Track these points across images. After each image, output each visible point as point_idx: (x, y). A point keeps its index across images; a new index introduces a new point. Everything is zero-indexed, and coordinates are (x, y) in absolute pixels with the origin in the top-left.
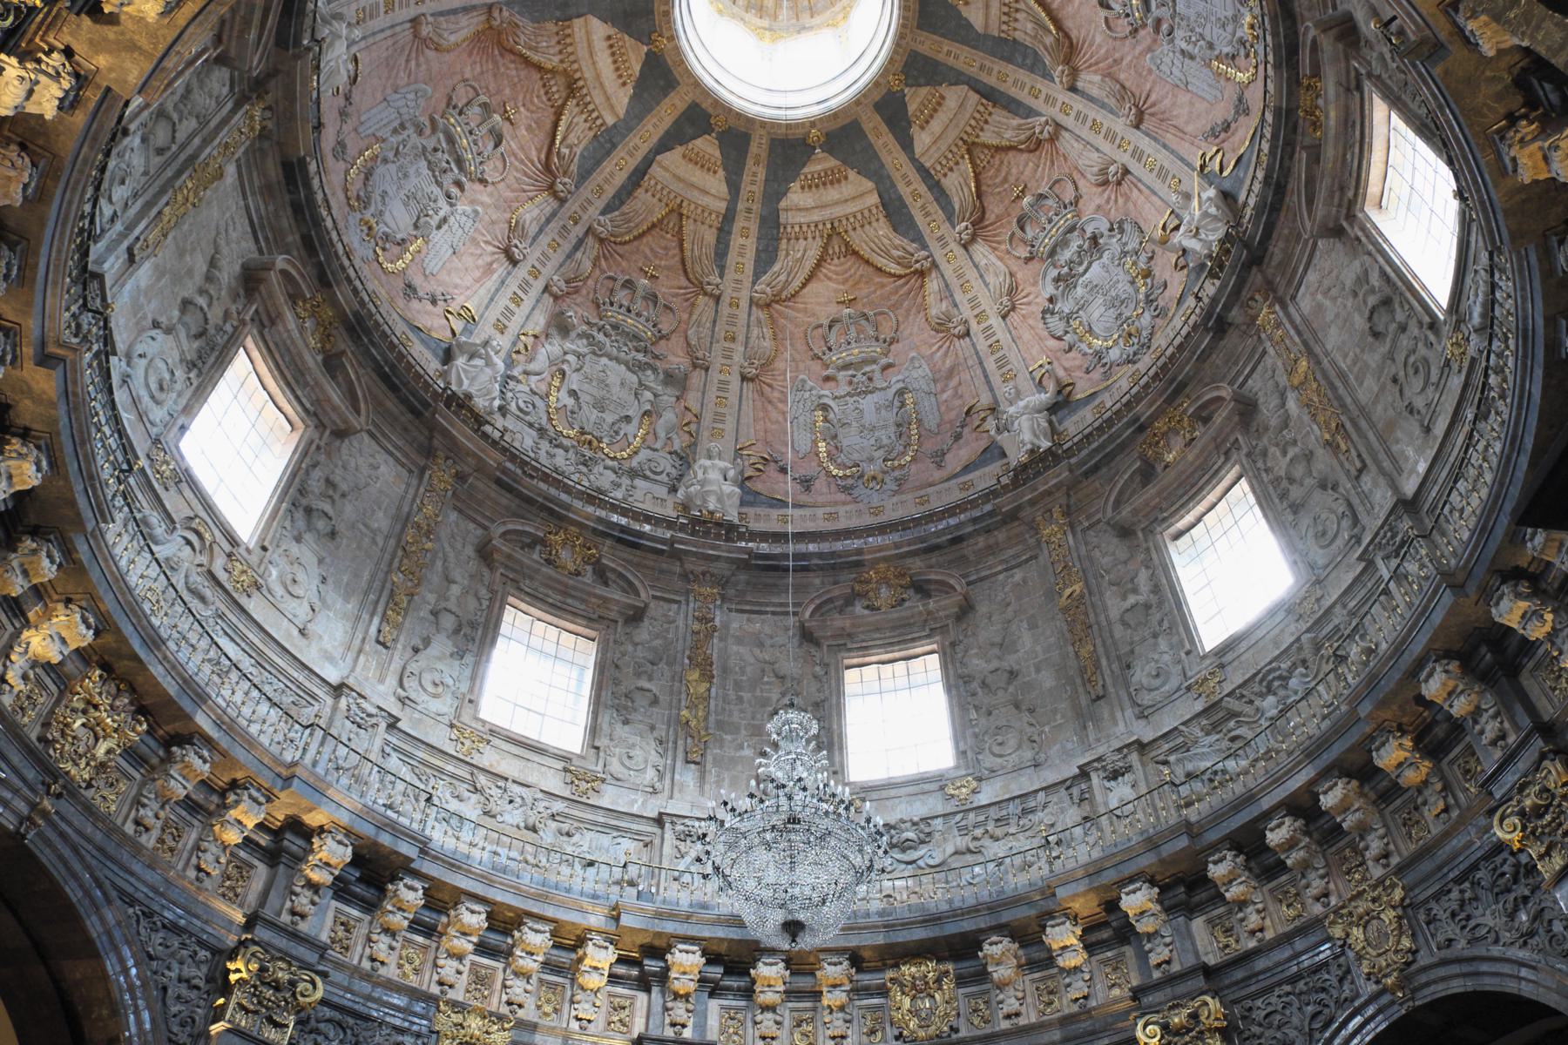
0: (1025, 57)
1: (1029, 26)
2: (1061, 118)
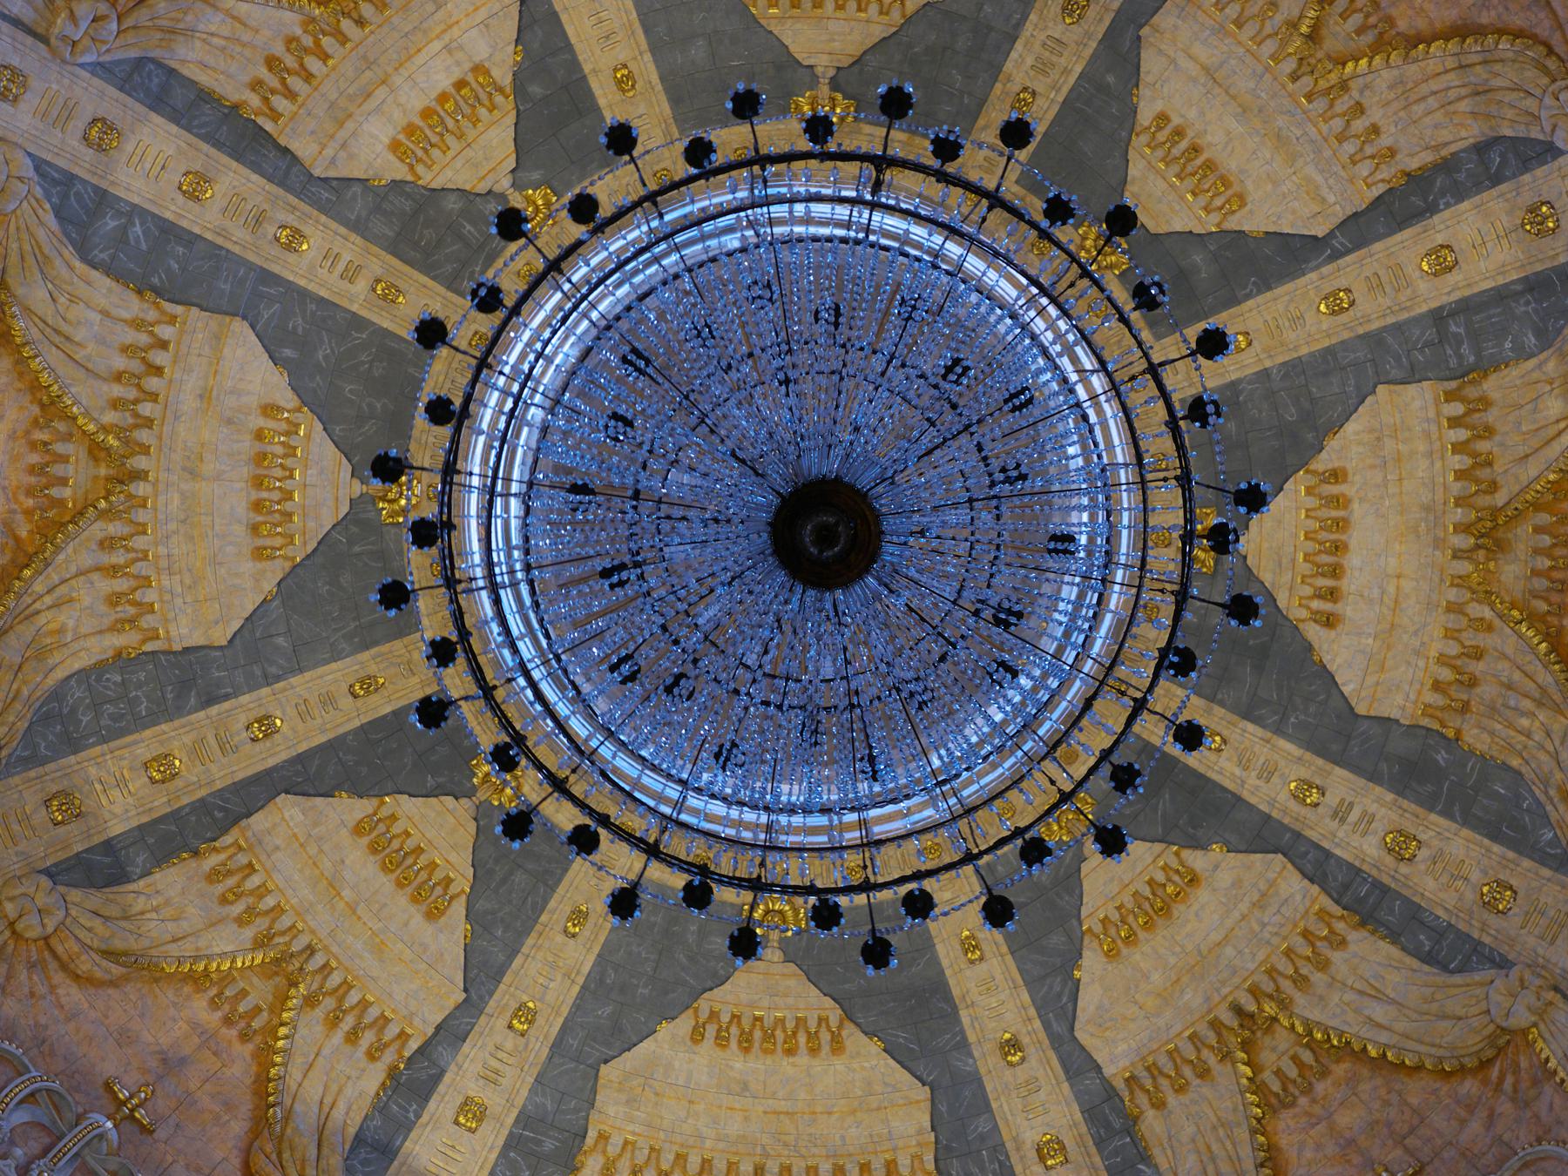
0: (121, 237)
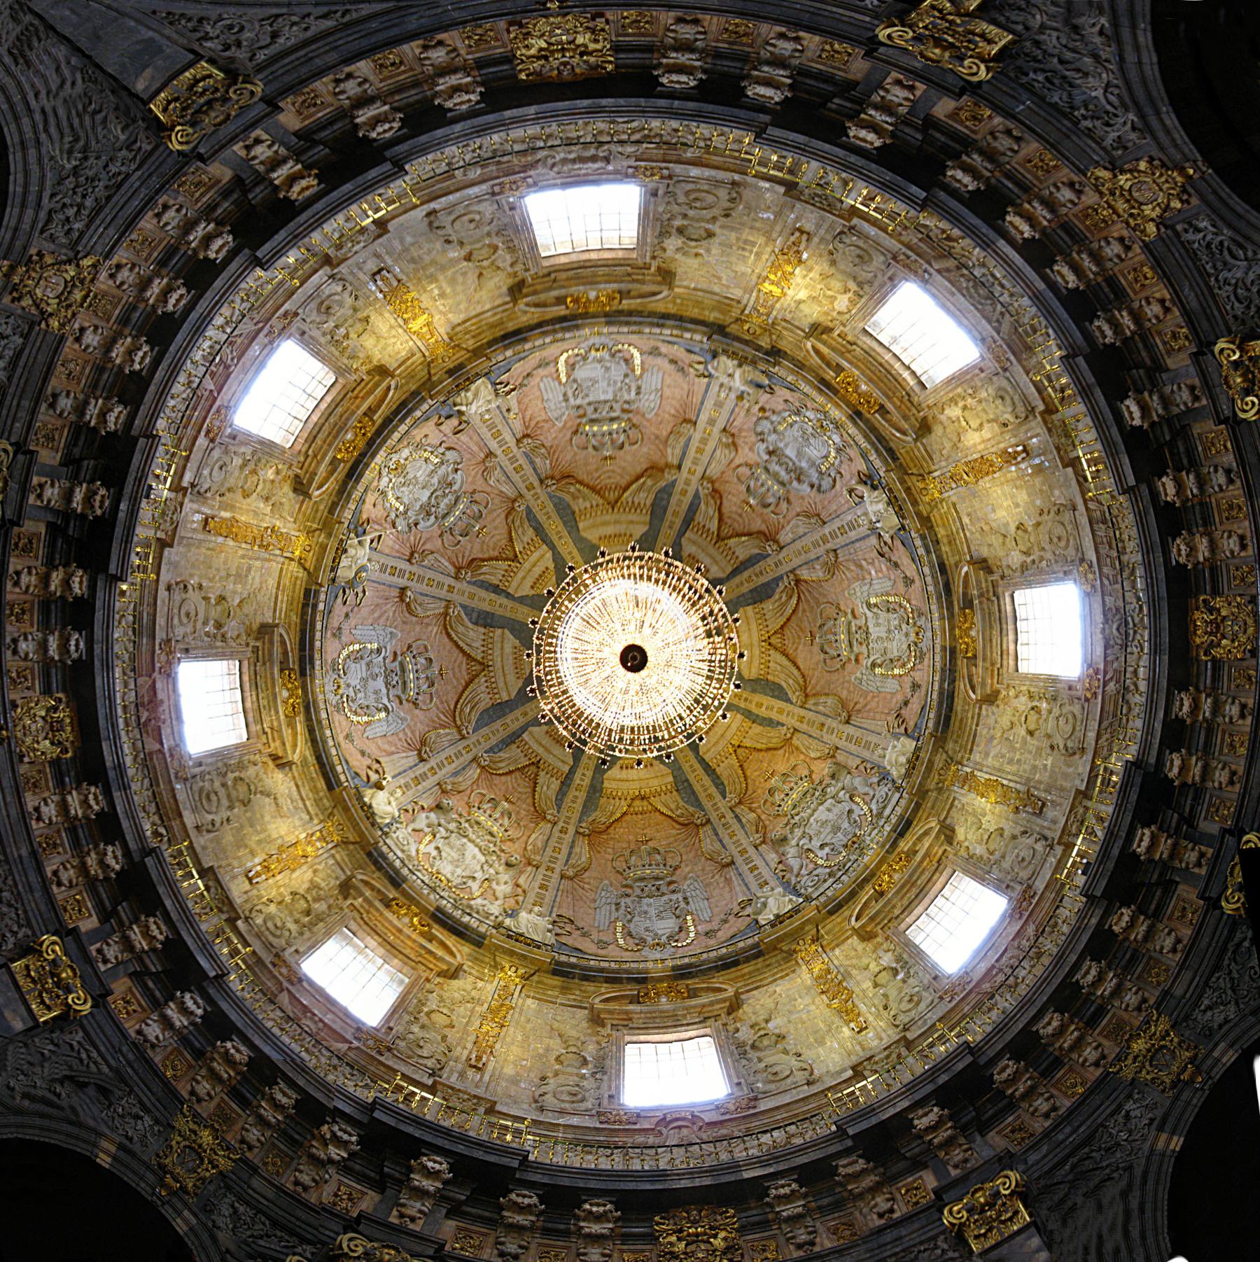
0: (662, 499)
1: (642, 495)
2: (699, 474)
